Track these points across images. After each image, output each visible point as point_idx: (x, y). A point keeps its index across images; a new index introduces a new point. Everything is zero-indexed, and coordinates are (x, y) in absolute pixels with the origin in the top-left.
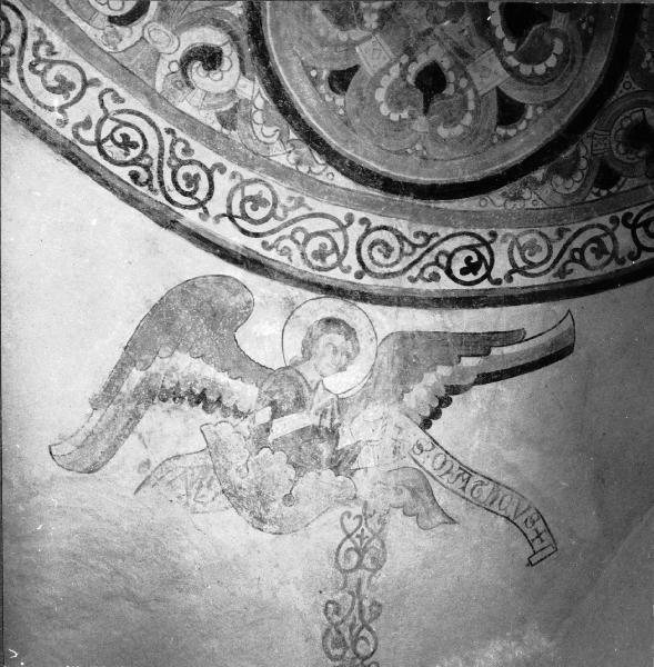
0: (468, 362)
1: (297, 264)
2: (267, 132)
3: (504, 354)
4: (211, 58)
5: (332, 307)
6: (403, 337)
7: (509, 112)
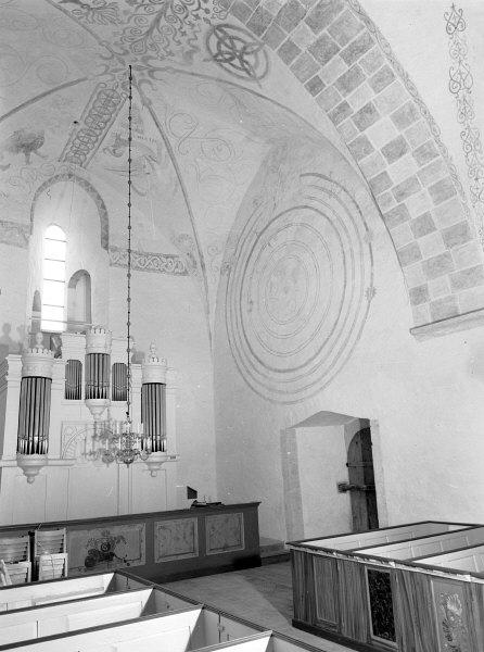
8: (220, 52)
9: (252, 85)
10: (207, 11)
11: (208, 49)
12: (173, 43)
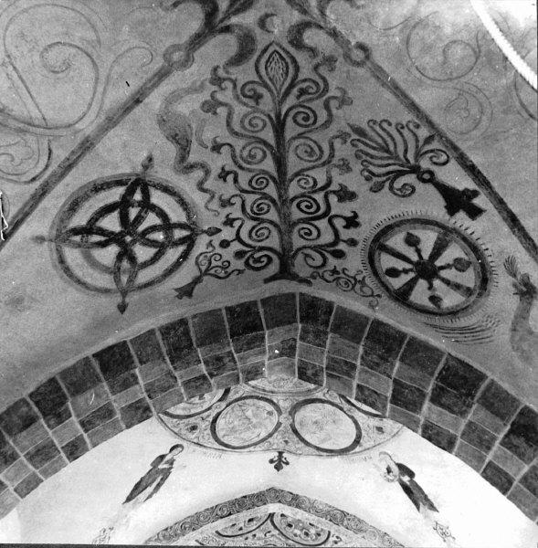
8: (147, 205)
9: (39, 224)
10: (225, 244)
11: (166, 190)
12: (224, 136)
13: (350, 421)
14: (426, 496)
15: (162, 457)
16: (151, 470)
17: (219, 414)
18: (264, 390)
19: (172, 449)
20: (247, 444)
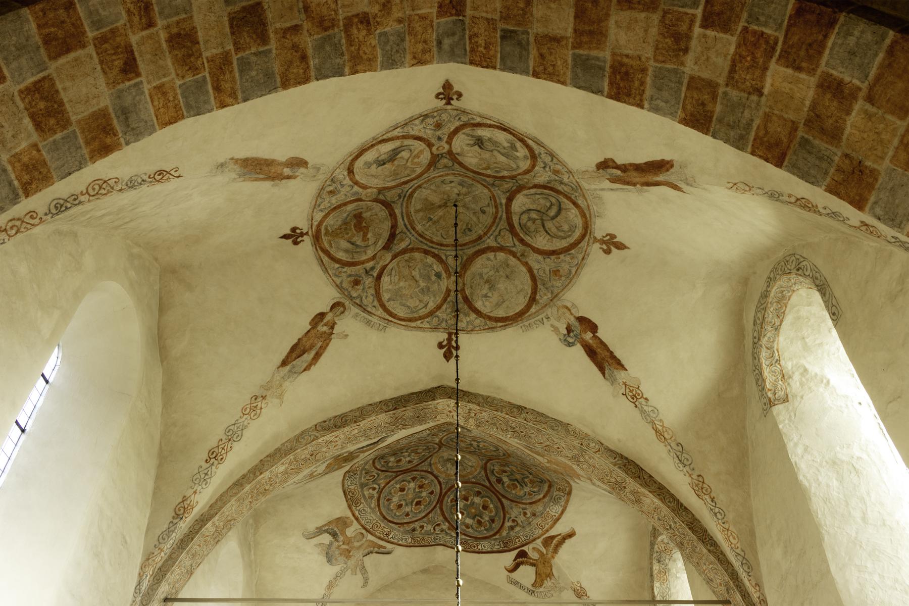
0: (376, 549)
1: (363, 522)
2: (374, 504)
3: (382, 550)
4: (374, 489)
5: (364, 531)
6: (370, 541)
7: (407, 515)
13: (524, 269)
14: (612, 353)
15: (322, 315)
16: (309, 331)
17: (384, 268)
18: (432, 242)
19: (332, 308)
20: (416, 315)
